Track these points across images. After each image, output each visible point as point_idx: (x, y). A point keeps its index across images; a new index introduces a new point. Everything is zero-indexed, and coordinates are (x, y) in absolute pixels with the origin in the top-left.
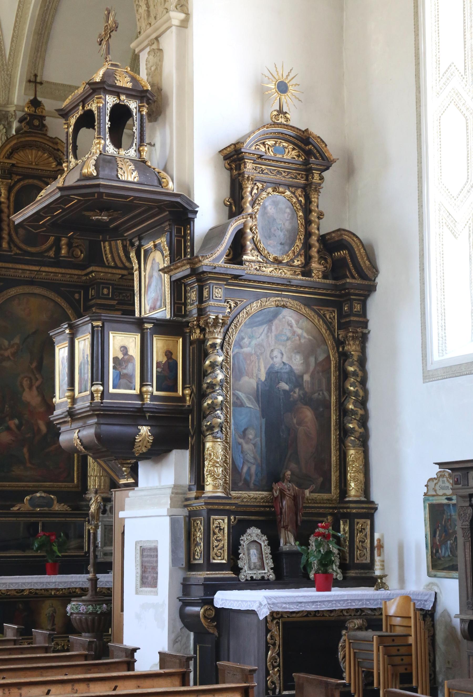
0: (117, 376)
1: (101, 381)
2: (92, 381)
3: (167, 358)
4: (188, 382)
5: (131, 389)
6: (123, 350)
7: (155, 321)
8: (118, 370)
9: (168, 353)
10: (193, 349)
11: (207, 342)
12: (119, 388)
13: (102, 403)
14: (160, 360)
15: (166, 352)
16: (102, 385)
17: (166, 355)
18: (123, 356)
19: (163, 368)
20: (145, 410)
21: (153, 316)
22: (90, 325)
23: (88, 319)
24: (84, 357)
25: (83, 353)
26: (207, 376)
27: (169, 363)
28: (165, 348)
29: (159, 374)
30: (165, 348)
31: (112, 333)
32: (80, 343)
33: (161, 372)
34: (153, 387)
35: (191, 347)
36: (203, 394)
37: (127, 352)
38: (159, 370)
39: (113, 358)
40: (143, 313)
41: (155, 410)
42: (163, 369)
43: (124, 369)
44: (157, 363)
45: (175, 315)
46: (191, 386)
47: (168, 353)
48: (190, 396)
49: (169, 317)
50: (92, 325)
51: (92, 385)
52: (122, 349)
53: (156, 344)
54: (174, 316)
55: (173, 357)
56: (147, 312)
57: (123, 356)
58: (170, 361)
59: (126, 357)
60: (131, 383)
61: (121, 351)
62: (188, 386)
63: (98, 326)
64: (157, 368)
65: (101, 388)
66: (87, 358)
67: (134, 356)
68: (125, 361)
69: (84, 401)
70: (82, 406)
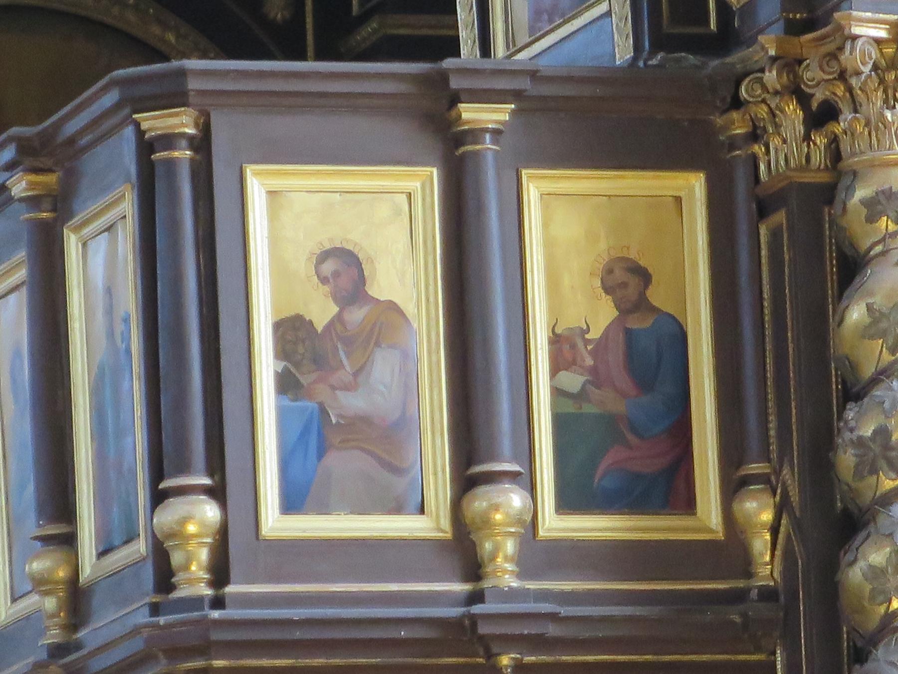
0: (305, 432)
1: (211, 473)
2: (157, 472)
3: (617, 307)
4: (753, 443)
5: (398, 509)
6: (336, 274)
7: (524, 84)
8: (310, 397)
9: (620, 275)
10: (776, 234)
11: (850, 189)
12: (323, 509)
13: (218, 603)
14: (572, 320)
15: (609, 271)
16: (217, 493)
17: (607, 290)
18: (335, 309)
19: (594, 371)
20: (484, 629)
21: (542, 62)
22: (129, 132)
23: (110, 99)
24: (111, 333)
25: (110, 311)
26: (858, 397)
27: (629, 334)
28: (603, 249)
29: (569, 407)
30: (603, 246)
31: (256, 174)
32: (92, 245)
33: (580, 397)
34: (532, 489)
35: (763, 230)
36: (845, 510)
37: (361, 280)
38: (573, 381)
39: (278, 326)
40: (500, 49)
41: (552, 630)
42: (597, 377)
43: (348, 388)
44: (556, 340)
45: (661, 42)
46: (778, 472)
47: (620, 275)
48: (775, 530)
49: (629, 55)
50: (140, 133)
51: (158, 497)
52: (328, 267)
53: (546, 225)
54: (656, 46)
55: (658, 296)
56: (523, 38)
57: (335, 309)
58: (637, 323)
59: (357, 315)
60: (397, 471)
61: (324, 280)
62: (755, 468)
63: (168, 140)
64: (555, 370)
65: (210, 512)
66: (127, 339)
67: (410, 309)
68: (348, 342)
69: (125, 601)
70: (118, 630)
